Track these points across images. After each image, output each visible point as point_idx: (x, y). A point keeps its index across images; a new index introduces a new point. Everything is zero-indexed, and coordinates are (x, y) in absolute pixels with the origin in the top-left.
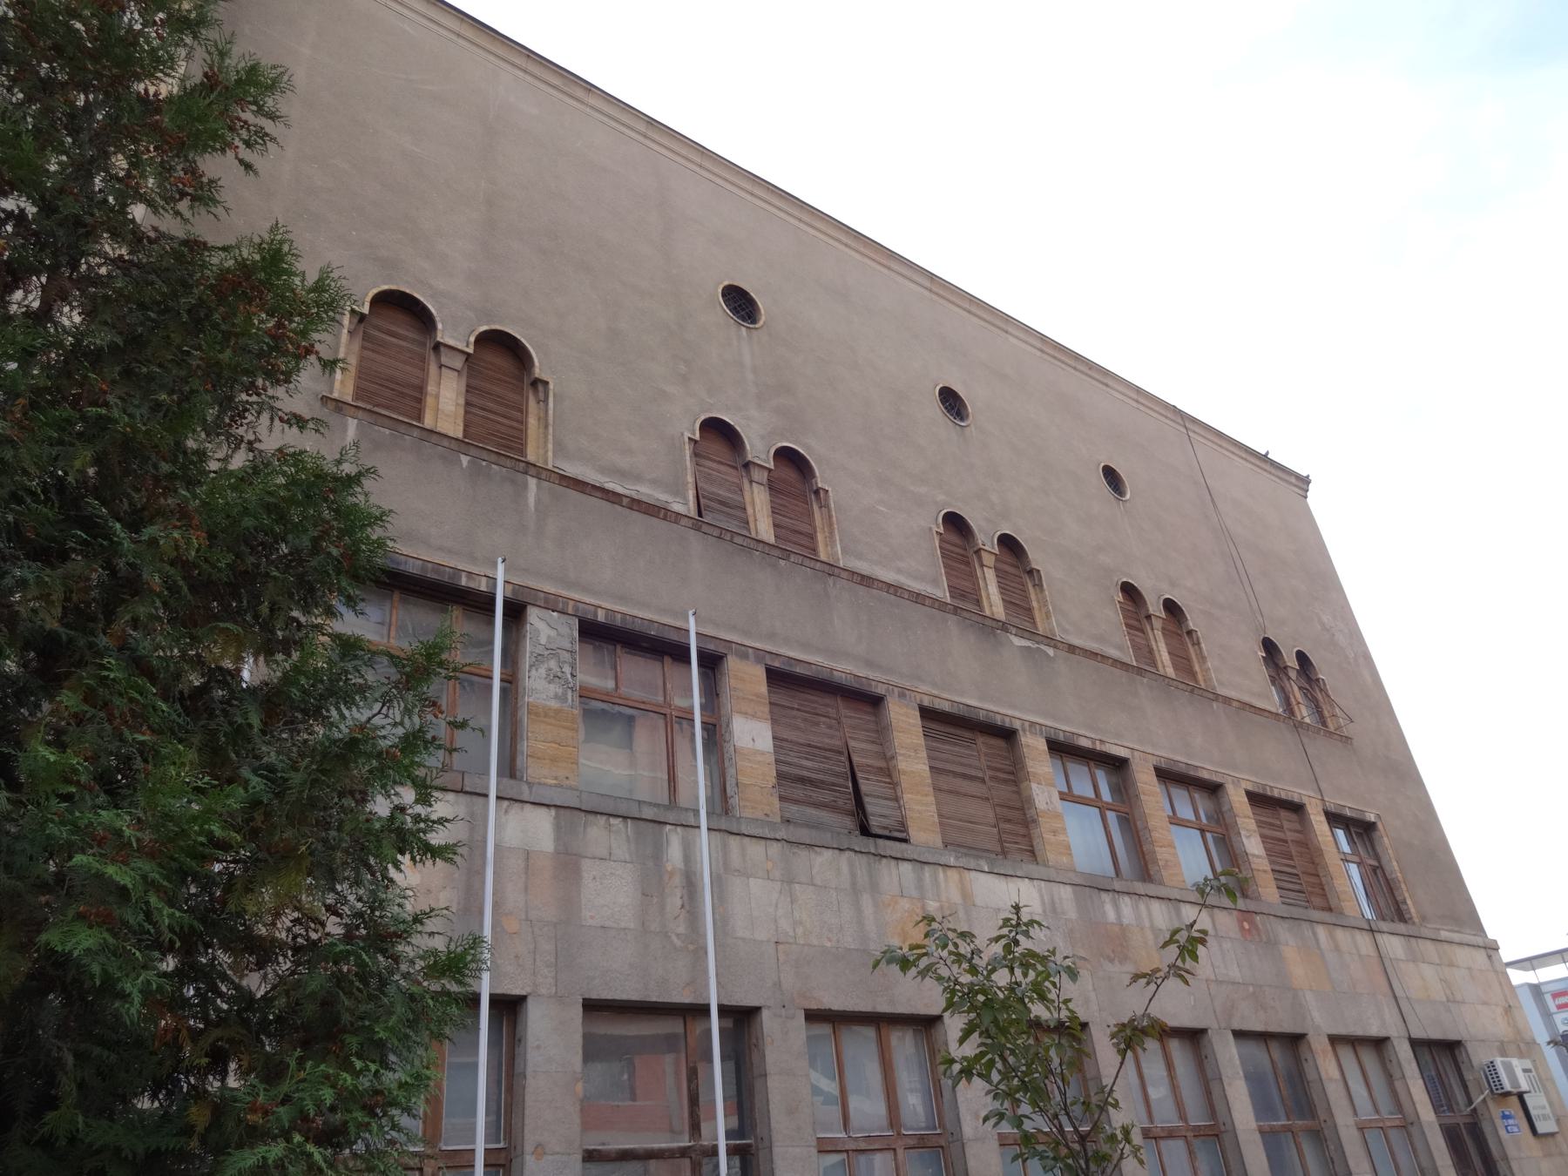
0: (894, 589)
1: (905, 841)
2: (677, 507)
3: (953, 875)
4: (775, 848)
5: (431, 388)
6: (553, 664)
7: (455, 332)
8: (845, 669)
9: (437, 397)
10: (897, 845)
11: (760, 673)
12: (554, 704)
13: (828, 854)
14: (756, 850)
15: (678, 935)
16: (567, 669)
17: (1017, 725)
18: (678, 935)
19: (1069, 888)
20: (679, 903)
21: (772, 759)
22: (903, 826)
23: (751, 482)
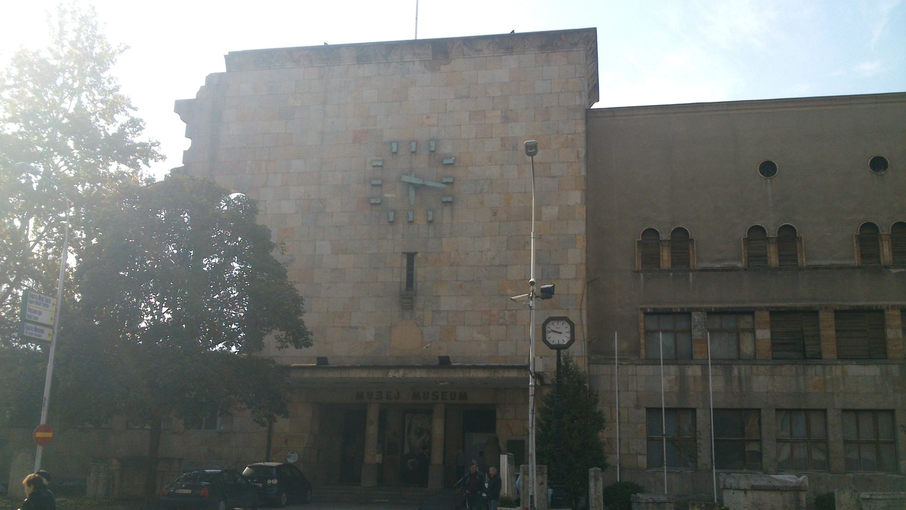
0: (830, 268)
1: (821, 358)
2: (740, 265)
3: (840, 367)
4: (768, 367)
5: (661, 254)
6: (699, 326)
7: (665, 236)
8: (799, 305)
9: (663, 256)
10: (818, 360)
11: (767, 314)
12: (700, 338)
13: (787, 366)
14: (762, 369)
15: (736, 393)
16: (704, 327)
17: (884, 308)
18: (736, 393)
19: (897, 366)
20: (737, 384)
21: (770, 341)
22: (820, 353)
23: (769, 244)
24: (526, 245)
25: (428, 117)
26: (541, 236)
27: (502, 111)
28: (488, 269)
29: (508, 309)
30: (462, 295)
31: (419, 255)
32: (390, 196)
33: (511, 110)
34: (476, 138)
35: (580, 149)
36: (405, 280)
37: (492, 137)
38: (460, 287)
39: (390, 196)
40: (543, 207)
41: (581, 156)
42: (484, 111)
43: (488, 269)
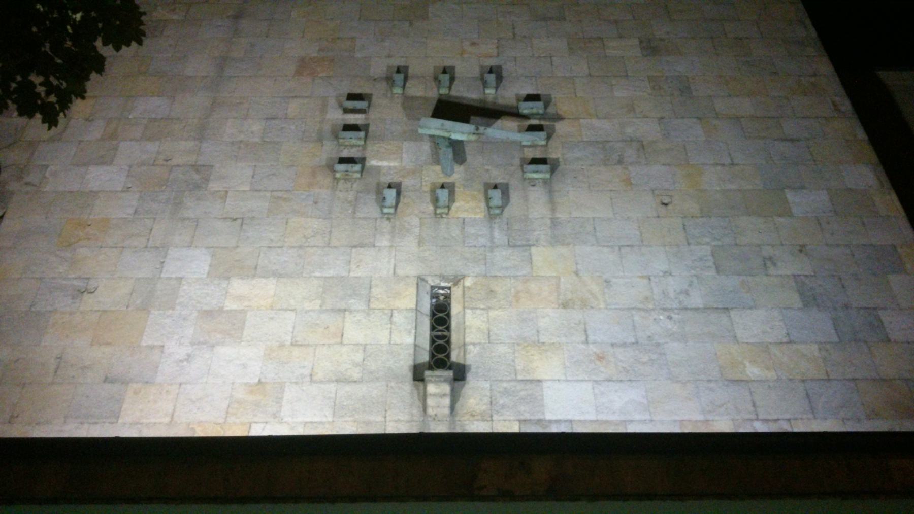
24: (769, 263)
25: (473, 44)
26: (803, 246)
27: (641, 42)
28: (675, 316)
29: (761, 417)
30: (609, 380)
31: (468, 282)
32: (385, 164)
33: (662, 40)
34: (590, 75)
35: (837, 99)
36: (425, 343)
37: (627, 76)
38: (600, 358)
39: (385, 164)
40: (786, 190)
41: (843, 108)
42: (602, 38)
43: (675, 316)
